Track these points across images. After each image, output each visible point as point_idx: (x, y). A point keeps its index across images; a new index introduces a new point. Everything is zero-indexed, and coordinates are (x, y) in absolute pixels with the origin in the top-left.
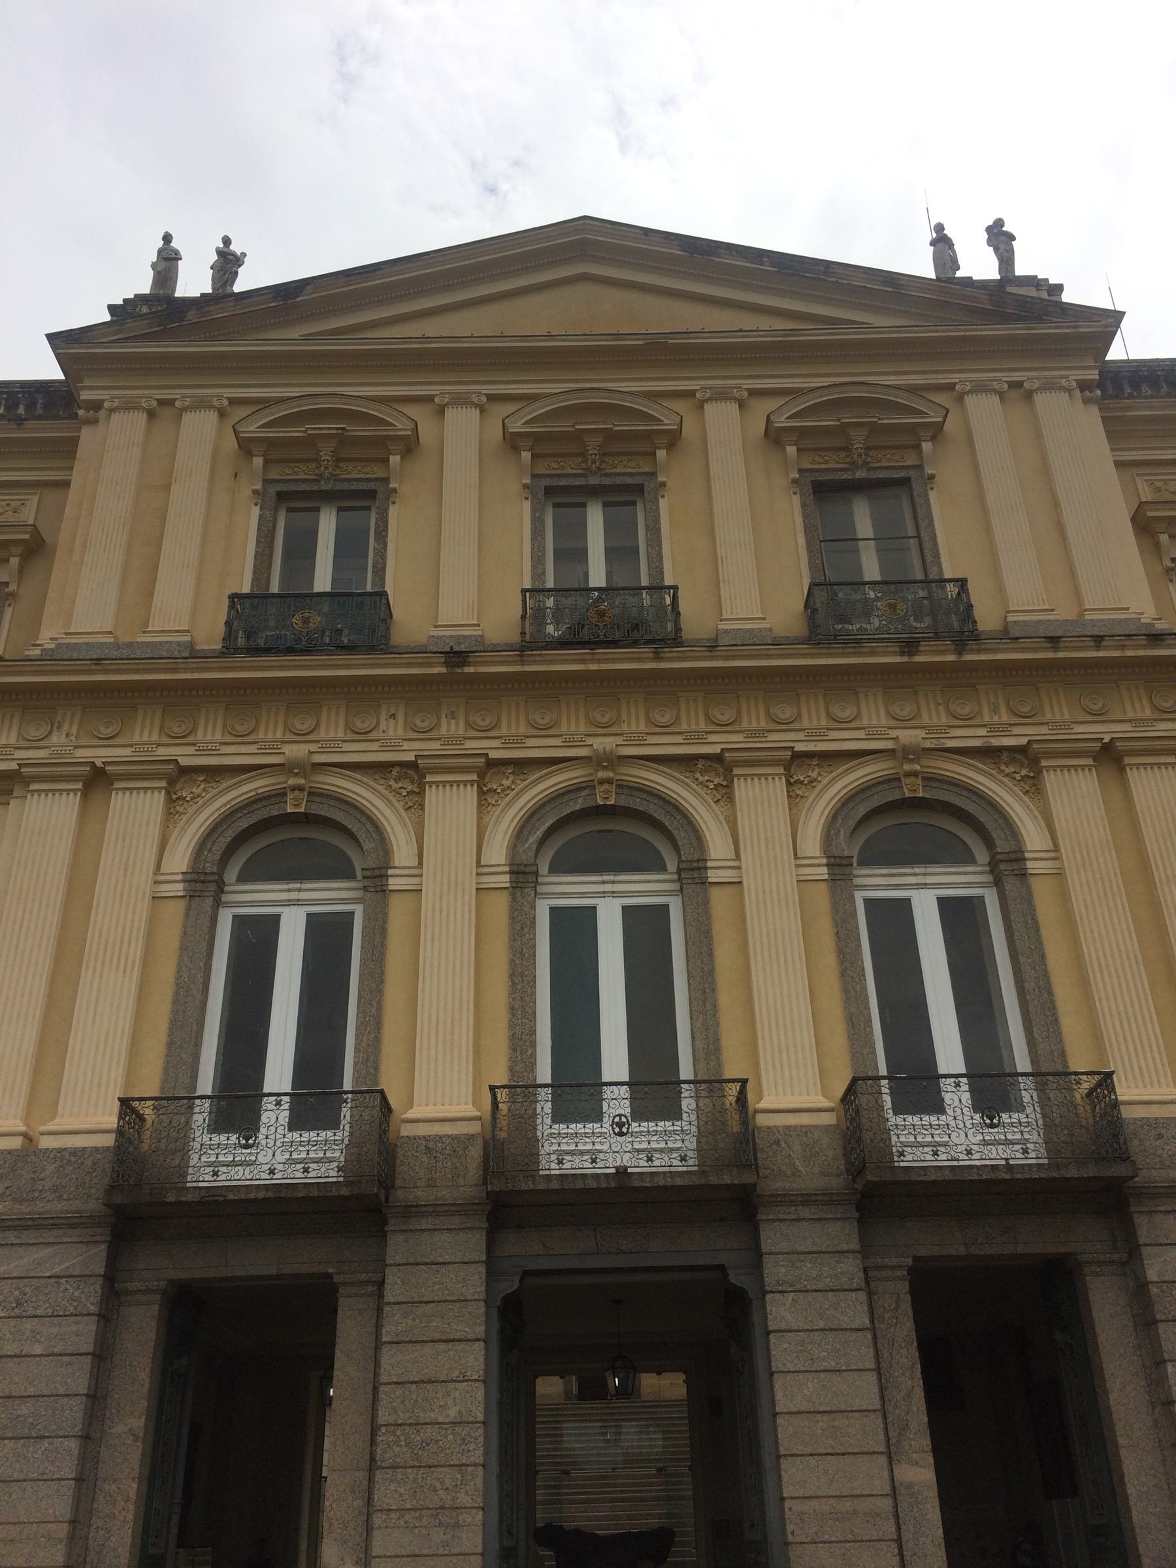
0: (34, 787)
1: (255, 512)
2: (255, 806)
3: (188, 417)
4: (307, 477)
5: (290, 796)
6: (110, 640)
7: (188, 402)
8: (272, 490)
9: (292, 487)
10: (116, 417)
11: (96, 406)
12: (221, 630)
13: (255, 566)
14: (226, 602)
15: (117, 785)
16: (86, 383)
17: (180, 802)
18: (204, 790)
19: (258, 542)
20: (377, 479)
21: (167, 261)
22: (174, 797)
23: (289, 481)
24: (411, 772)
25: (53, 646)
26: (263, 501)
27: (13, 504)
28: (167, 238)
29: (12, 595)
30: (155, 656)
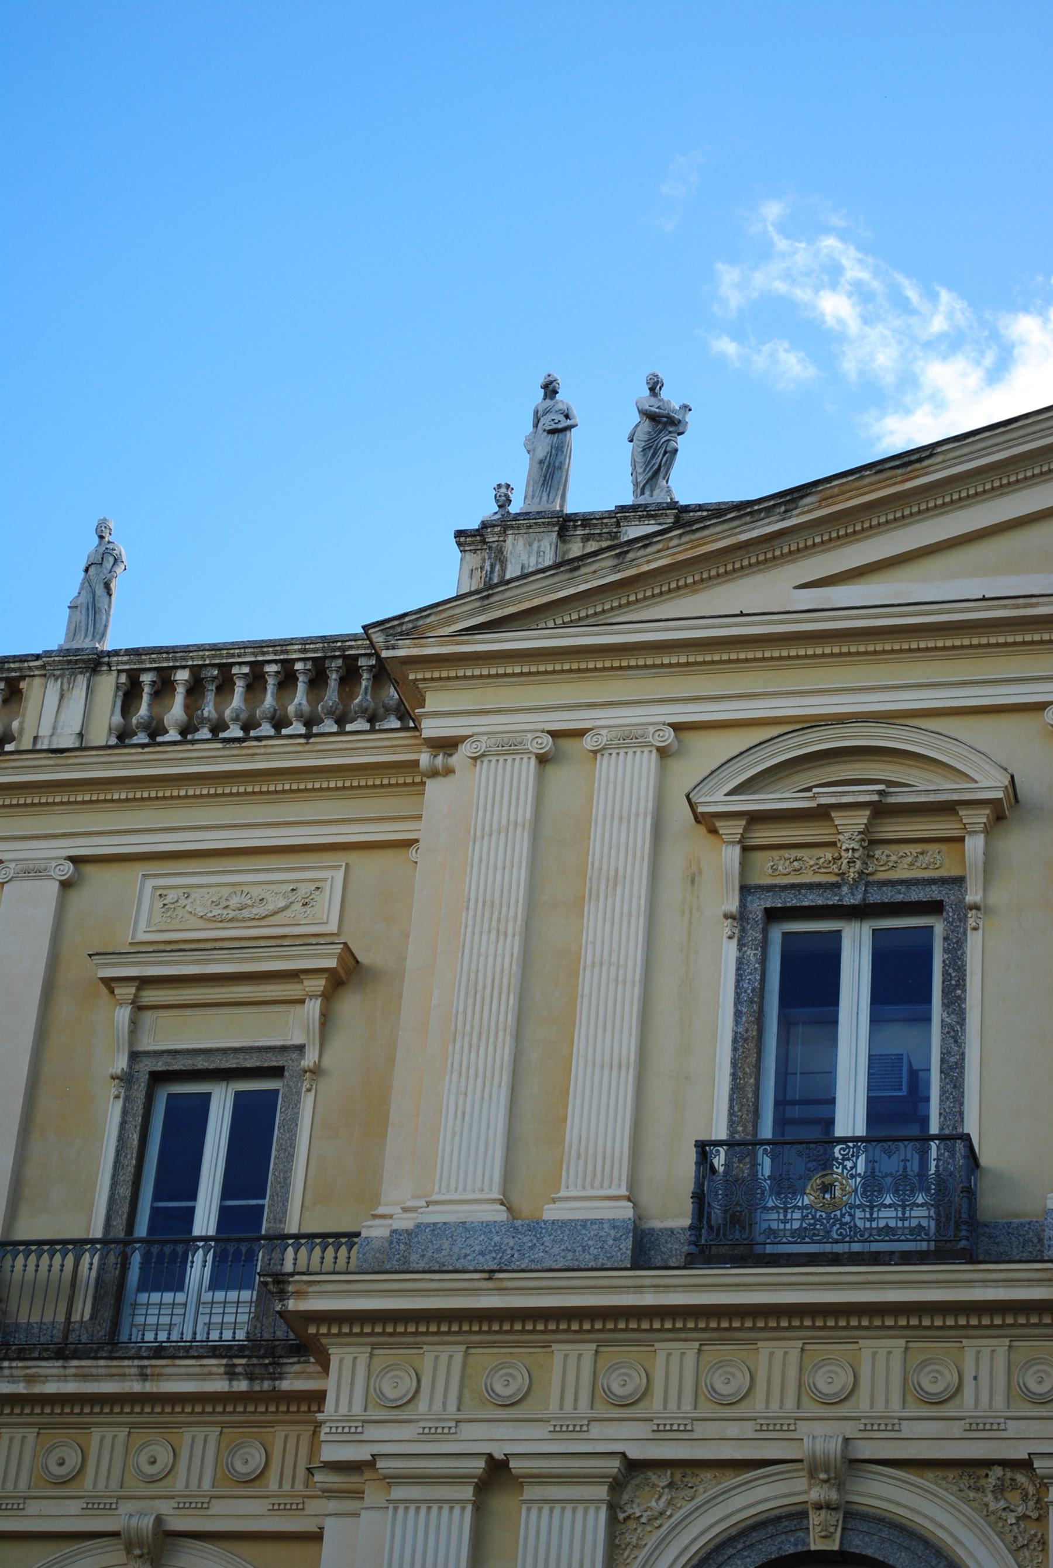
0: (399, 1492)
1: (730, 951)
2: (755, 1536)
3: (605, 765)
4: (817, 879)
5: (815, 1519)
6: (500, 1215)
7: (604, 737)
8: (758, 906)
9: (792, 900)
10: (483, 768)
11: (448, 745)
12: (688, 1205)
13: (734, 1064)
14: (691, 1155)
15: (530, 1492)
16: (434, 701)
17: (632, 1524)
18: (669, 1503)
19: (738, 1014)
20: (943, 881)
21: (554, 430)
22: (621, 1516)
23: (785, 888)
24: (1021, 1478)
25: (409, 1225)
26: (743, 930)
27: (304, 889)
28: (550, 389)
29: (316, 1072)
30: (577, 1248)
